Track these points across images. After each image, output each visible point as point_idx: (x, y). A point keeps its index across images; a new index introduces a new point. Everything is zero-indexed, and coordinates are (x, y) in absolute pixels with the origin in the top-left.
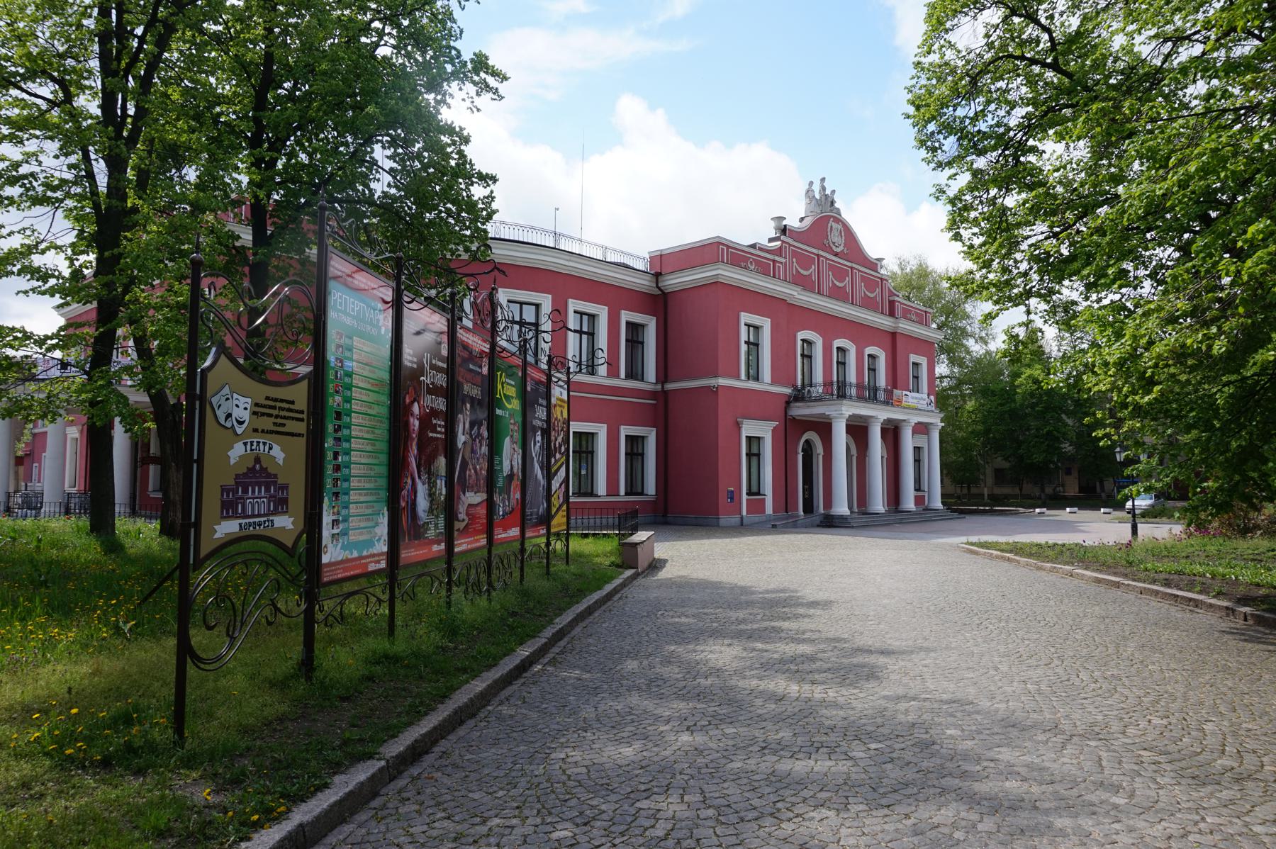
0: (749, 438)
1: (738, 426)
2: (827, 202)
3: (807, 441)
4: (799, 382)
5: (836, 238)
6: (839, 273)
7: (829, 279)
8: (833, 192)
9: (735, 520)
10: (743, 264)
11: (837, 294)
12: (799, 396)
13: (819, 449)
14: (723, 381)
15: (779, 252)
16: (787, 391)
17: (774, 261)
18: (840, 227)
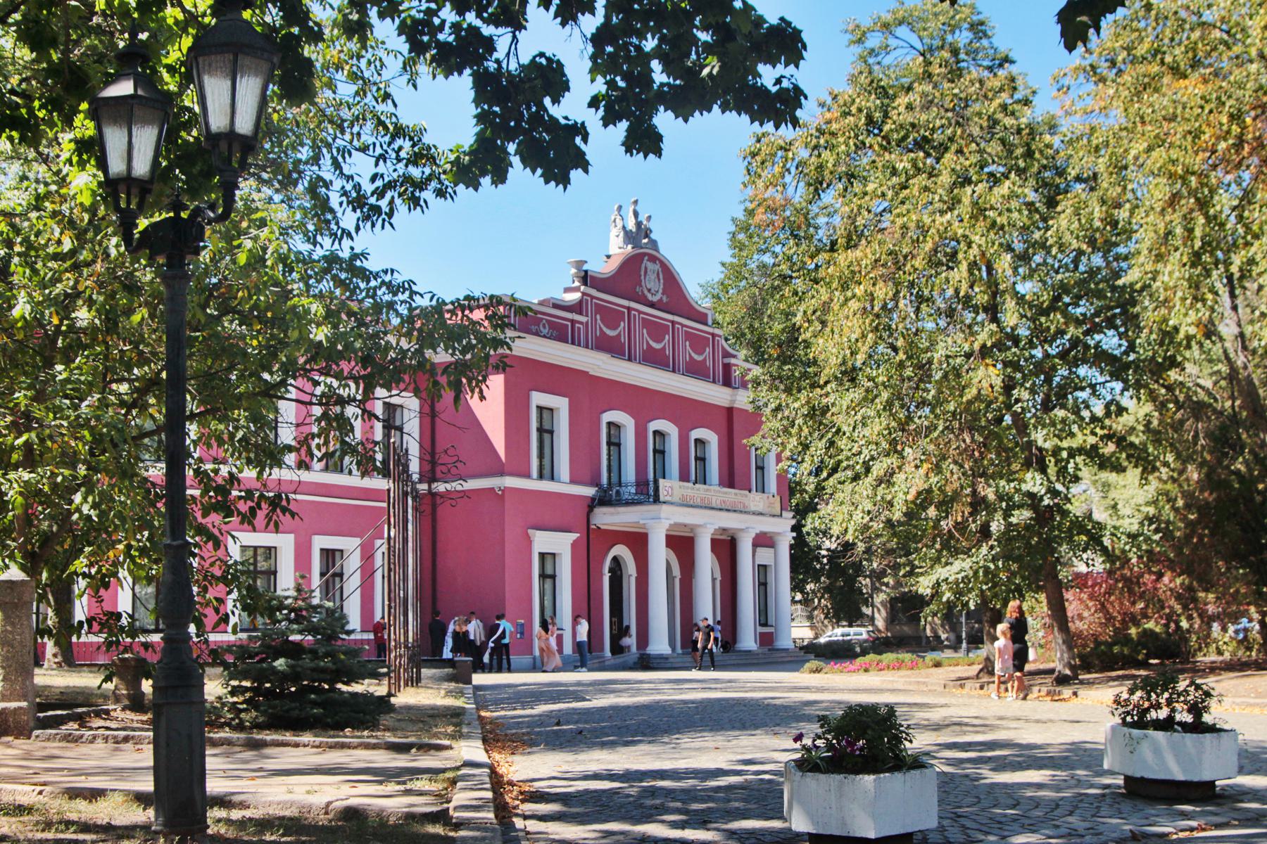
0: (543, 556)
1: (529, 542)
2: (639, 235)
3: (615, 559)
4: (605, 480)
5: (652, 285)
6: (657, 330)
7: (644, 339)
8: (649, 218)
9: (526, 659)
10: (534, 328)
11: (655, 359)
12: (605, 499)
13: (631, 568)
14: (511, 482)
15: (577, 308)
16: (590, 491)
17: (573, 322)
18: (657, 267)
